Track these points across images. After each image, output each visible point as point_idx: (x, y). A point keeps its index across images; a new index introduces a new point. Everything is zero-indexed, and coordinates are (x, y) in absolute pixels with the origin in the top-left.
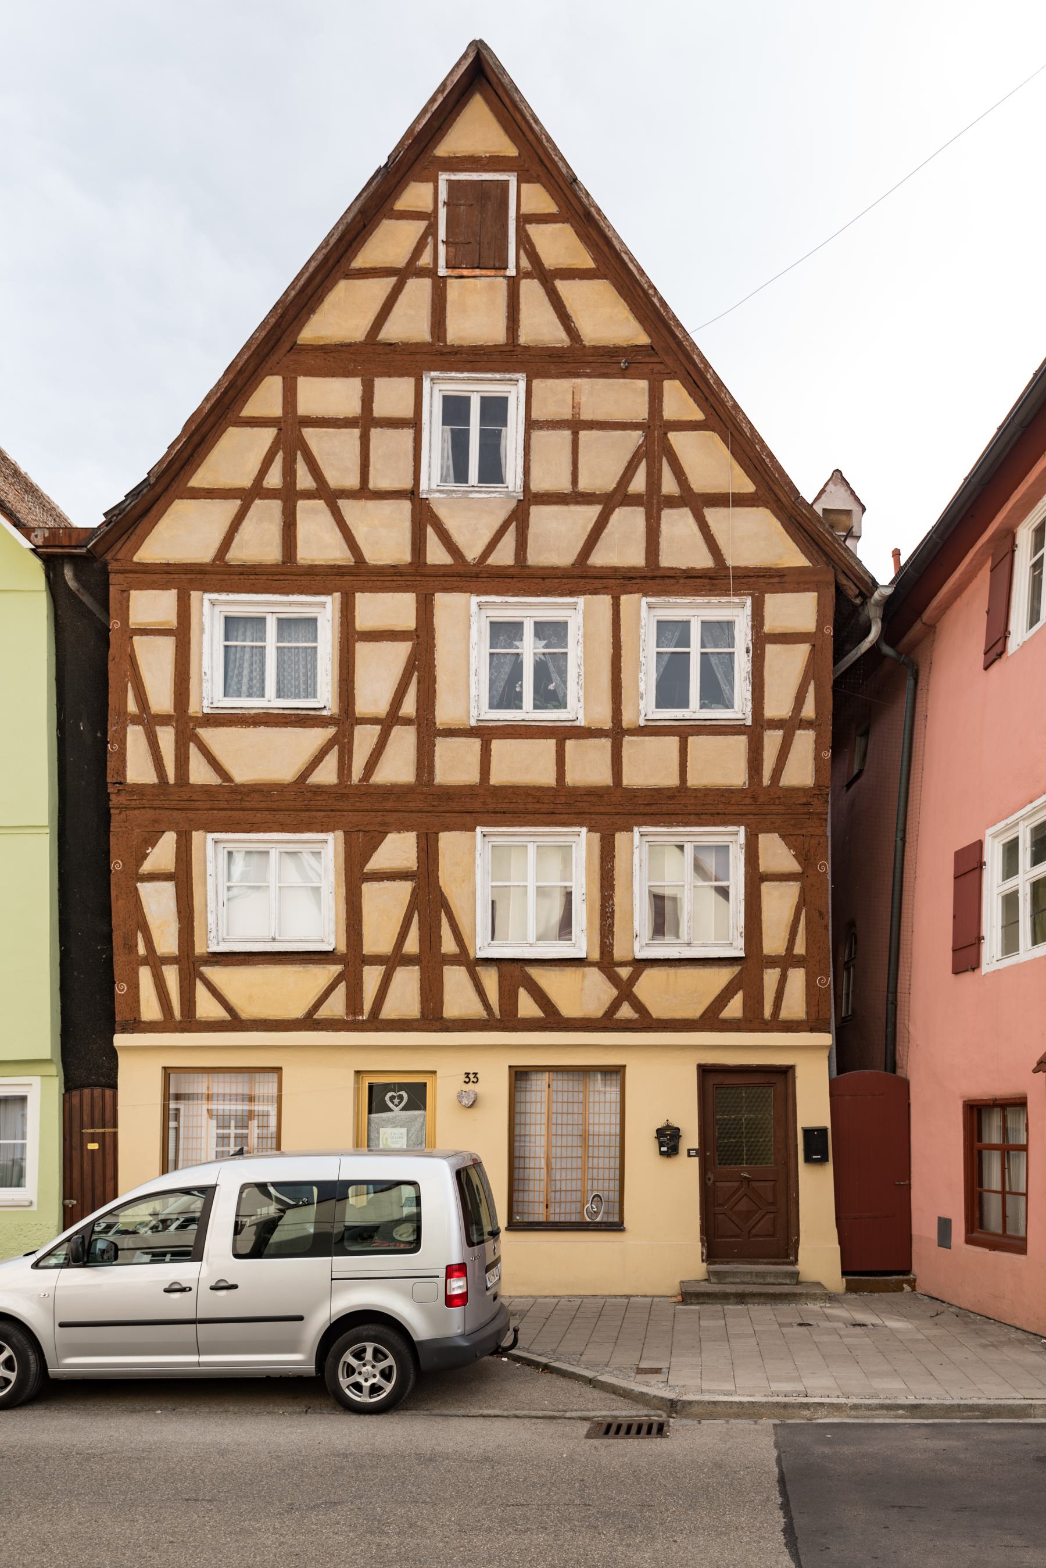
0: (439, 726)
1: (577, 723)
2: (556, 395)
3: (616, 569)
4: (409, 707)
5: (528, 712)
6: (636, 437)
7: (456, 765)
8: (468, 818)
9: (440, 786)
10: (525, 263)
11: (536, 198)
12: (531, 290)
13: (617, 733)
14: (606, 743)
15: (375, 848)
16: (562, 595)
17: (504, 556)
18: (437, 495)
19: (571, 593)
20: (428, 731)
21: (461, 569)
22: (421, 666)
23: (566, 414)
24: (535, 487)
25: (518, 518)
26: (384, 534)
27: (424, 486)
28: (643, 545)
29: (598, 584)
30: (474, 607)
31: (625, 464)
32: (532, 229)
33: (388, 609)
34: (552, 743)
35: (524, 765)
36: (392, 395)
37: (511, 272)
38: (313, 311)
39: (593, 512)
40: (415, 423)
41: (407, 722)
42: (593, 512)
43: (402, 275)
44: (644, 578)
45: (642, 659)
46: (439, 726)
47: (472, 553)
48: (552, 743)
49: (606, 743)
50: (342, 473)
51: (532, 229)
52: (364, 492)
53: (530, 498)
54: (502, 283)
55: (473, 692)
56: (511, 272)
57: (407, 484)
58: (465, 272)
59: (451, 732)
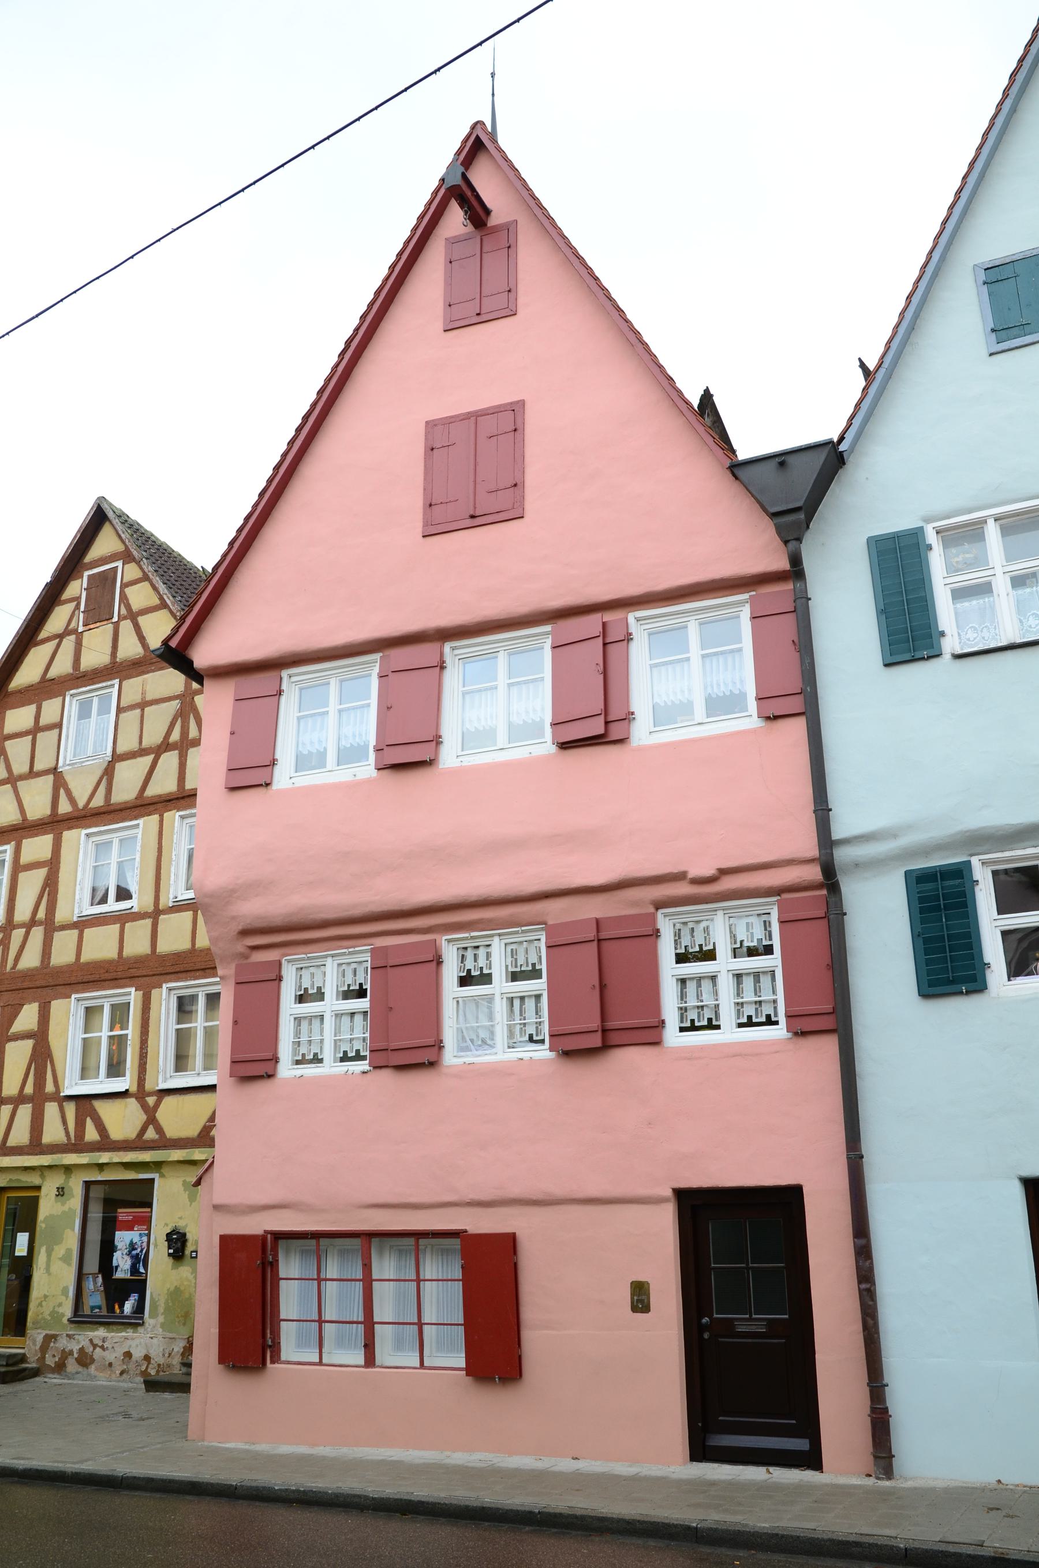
0: (57, 925)
1: (133, 910)
2: (134, 688)
3: (160, 796)
4: (41, 914)
5: (113, 906)
6: (175, 704)
7: (64, 951)
8: (68, 989)
9: (55, 968)
10: (124, 611)
11: (132, 571)
12: (126, 626)
13: (156, 914)
14: (148, 922)
15: (15, 1015)
16: (131, 820)
17: (98, 801)
18: (67, 768)
19: (136, 818)
20: (51, 927)
21: (76, 814)
22: (51, 885)
23: (138, 699)
24: (120, 750)
25: (109, 772)
26: (37, 800)
27: (60, 763)
28: (176, 776)
29: (152, 808)
30: (83, 837)
31: (168, 724)
32: (127, 590)
33: (38, 847)
34: (117, 927)
35: (100, 945)
36: (50, 709)
37: (115, 619)
38: (17, 670)
39: (149, 759)
40: (59, 726)
41: (40, 923)
42: (149, 759)
43: (60, 637)
44: (177, 799)
45: (174, 857)
46: (57, 925)
47: (81, 804)
48: (117, 927)
49: (148, 922)
50: (20, 766)
51: (127, 590)
52: (32, 774)
53: (117, 758)
54: (110, 627)
55: (77, 897)
56: (115, 619)
57: (52, 765)
58: (92, 626)
59: (63, 927)
